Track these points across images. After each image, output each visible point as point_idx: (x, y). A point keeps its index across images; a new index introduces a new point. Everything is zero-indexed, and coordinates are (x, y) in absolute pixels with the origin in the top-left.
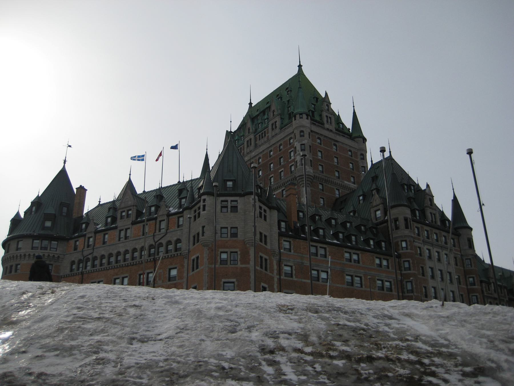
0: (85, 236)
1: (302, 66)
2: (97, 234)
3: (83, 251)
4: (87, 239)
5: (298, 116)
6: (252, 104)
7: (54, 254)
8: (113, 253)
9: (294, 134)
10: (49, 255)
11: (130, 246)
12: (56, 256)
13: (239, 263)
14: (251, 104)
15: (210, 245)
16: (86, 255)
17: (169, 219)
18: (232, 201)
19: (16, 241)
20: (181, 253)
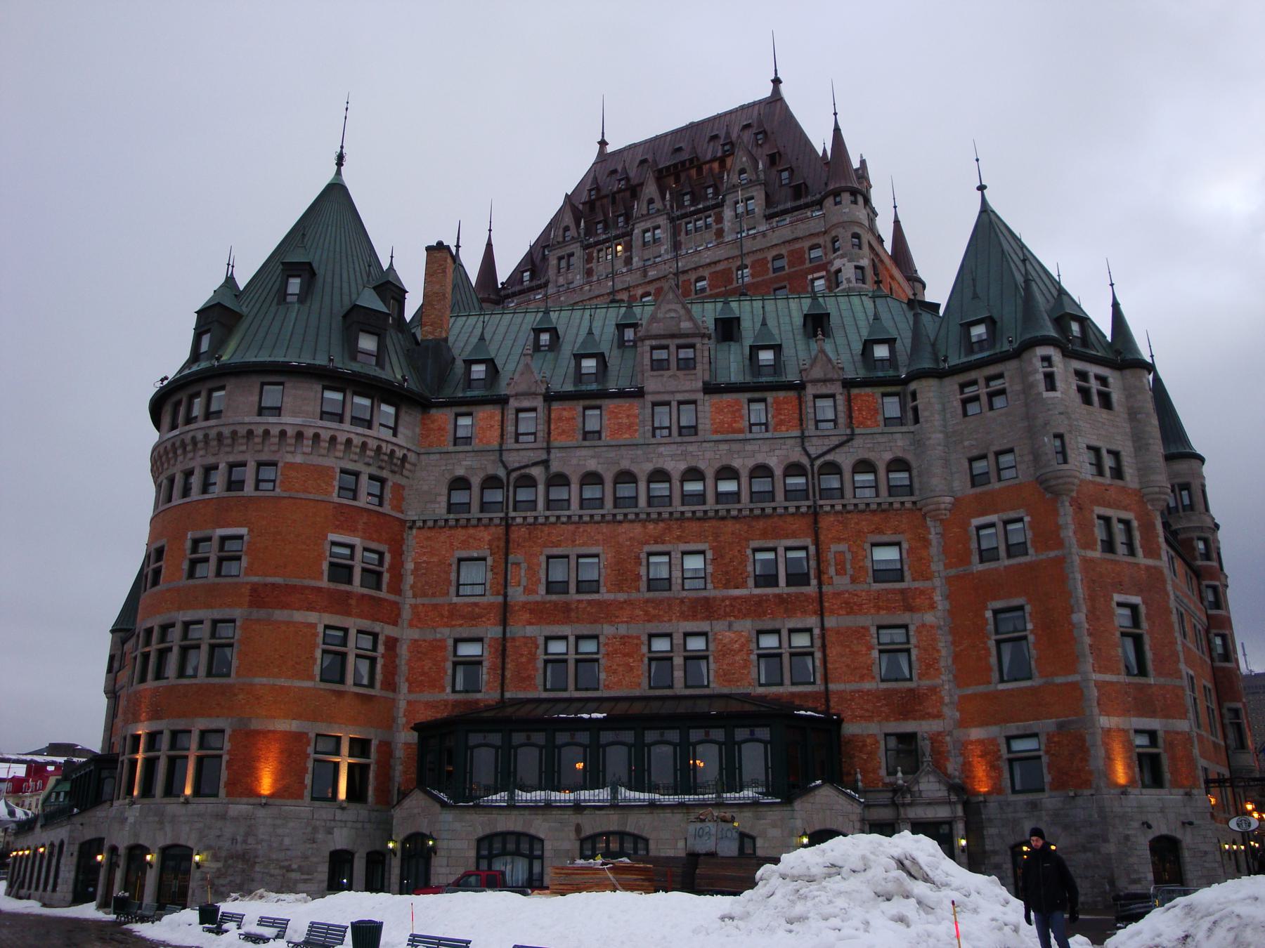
0: (502, 401)
1: (781, 82)
2: (554, 403)
3: (501, 451)
4: (510, 415)
5: (846, 197)
6: (607, 144)
7: (396, 449)
8: (635, 469)
9: (828, 238)
10: (379, 448)
11: (708, 460)
12: (399, 453)
13: (1140, 552)
14: (603, 143)
15: (1072, 491)
16: (516, 465)
17: (849, 396)
18: (1097, 377)
19: (256, 381)
20: (914, 503)
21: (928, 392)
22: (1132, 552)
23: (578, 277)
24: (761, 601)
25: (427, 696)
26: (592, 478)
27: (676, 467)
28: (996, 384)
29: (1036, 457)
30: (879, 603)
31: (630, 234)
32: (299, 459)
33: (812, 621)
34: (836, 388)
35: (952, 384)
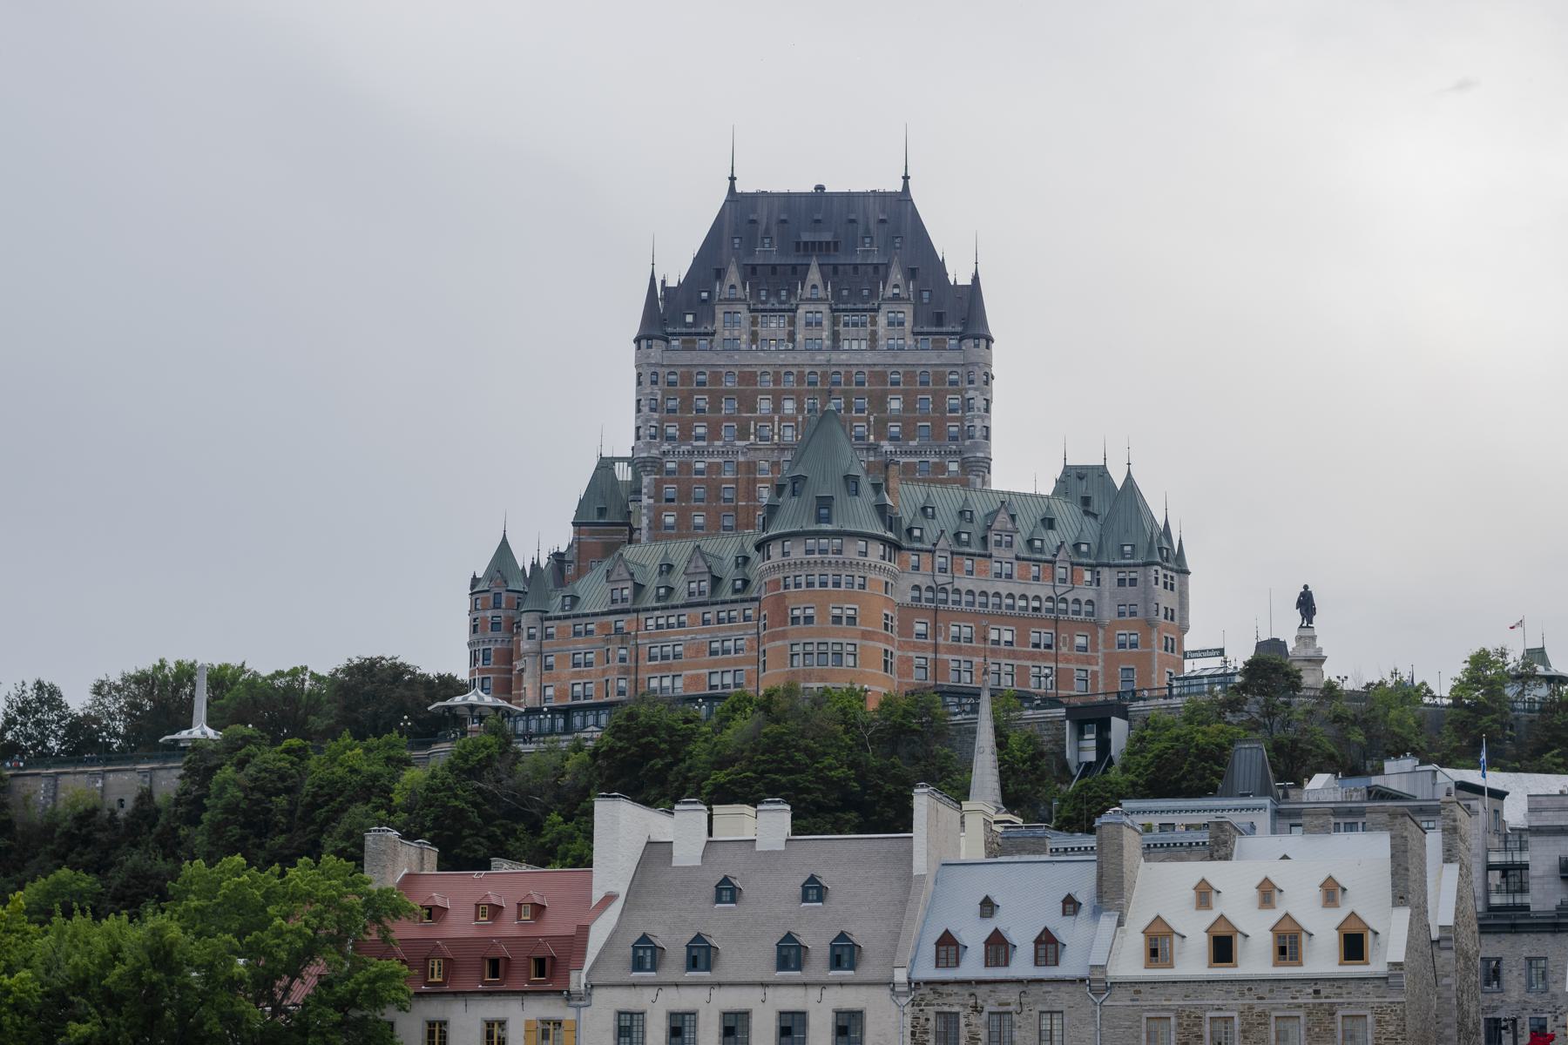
0: (932, 552)
11: (1017, 591)
21: (1106, 574)
22: (1173, 651)
23: (745, 337)
24: (1034, 653)
25: (906, 680)
26: (970, 592)
27: (1004, 593)
28: (1133, 575)
29: (1147, 611)
30: (1078, 660)
31: (794, 311)
32: (873, 576)
33: (1053, 665)
34: (1068, 565)
35: (1115, 570)
